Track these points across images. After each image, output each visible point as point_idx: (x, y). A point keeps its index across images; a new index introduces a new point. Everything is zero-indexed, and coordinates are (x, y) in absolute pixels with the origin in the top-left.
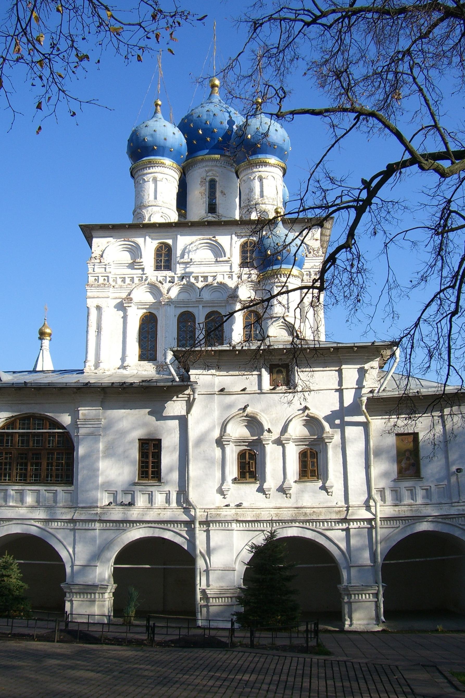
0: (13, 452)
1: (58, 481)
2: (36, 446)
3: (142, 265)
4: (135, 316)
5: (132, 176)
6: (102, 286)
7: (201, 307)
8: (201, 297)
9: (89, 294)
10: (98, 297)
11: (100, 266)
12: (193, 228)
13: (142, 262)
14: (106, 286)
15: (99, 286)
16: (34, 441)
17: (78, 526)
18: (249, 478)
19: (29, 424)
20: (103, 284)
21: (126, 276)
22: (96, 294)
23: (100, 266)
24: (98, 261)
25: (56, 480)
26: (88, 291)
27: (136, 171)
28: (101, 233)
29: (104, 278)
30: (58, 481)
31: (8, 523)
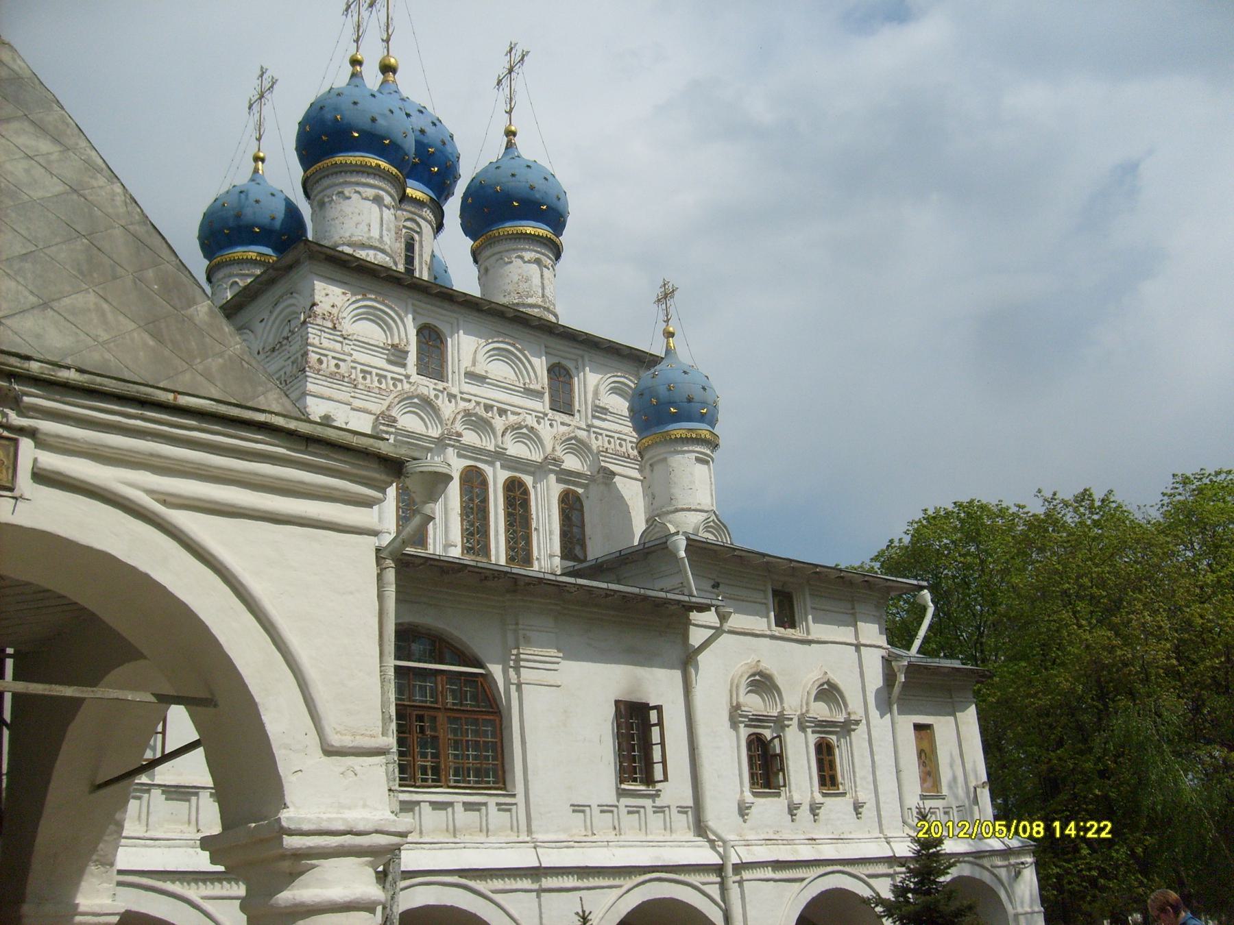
1: (488, 782)
7: (498, 464)
9: (310, 387)
10: (329, 399)
17: (549, 882)
21: (374, 371)
22: (327, 392)
24: (330, 325)
30: (488, 782)
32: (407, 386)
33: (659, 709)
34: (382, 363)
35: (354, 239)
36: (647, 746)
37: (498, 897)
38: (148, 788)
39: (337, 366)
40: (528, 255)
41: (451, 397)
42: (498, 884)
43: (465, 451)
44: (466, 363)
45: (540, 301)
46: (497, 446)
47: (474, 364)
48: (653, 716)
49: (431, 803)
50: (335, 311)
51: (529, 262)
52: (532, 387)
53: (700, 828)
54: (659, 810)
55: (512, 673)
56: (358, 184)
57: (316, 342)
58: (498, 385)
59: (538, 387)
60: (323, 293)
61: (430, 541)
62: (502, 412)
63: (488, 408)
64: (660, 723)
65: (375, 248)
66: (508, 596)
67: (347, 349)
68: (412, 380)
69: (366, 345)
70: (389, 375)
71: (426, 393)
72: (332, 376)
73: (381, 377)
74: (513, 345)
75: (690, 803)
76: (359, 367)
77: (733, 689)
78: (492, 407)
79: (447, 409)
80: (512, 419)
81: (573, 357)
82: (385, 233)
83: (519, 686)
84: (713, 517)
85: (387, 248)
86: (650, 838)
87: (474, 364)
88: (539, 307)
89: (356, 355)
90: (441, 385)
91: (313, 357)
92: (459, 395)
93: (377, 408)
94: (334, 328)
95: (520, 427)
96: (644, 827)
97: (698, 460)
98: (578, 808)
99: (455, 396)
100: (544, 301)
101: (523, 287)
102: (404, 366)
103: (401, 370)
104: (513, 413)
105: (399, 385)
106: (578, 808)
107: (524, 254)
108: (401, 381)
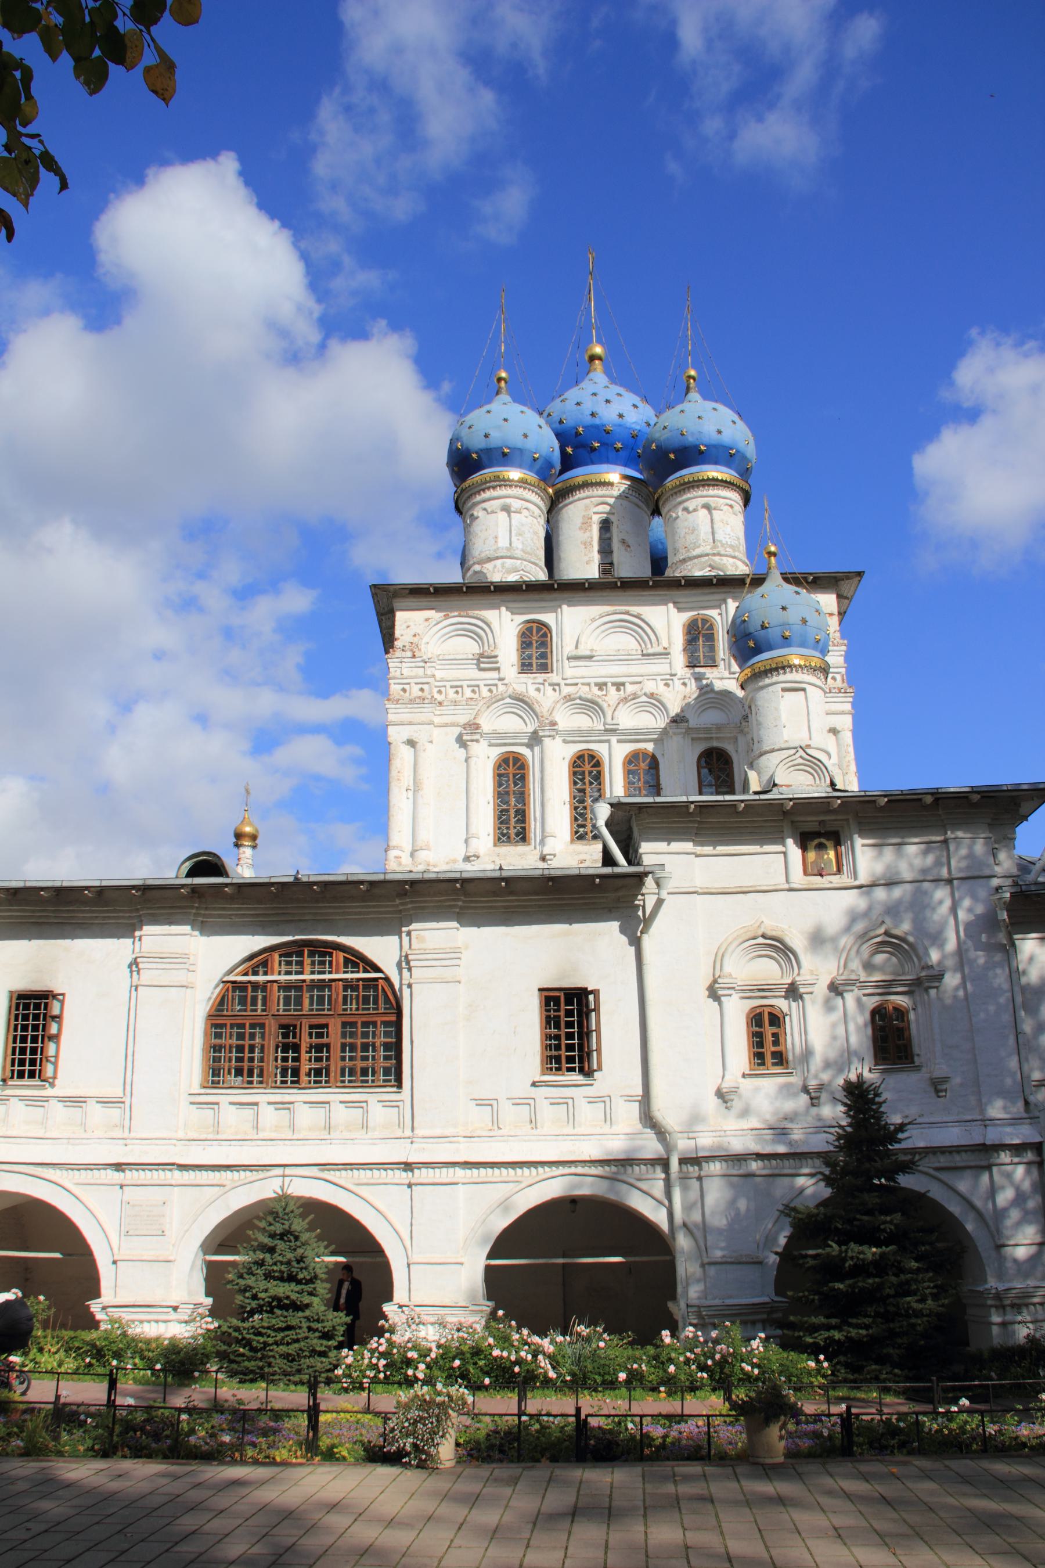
0: (267, 1022)
2: (317, 1010)
3: (497, 662)
4: (485, 758)
5: (459, 510)
6: (418, 701)
8: (614, 722)
9: (391, 717)
10: (410, 724)
11: (413, 665)
12: (591, 594)
13: (496, 657)
14: (426, 701)
15: (411, 701)
16: (311, 997)
18: (774, 1064)
19: (301, 963)
20: (419, 697)
21: (465, 684)
22: (406, 717)
23: (413, 665)
24: (409, 654)
25: (362, 1081)
26: (390, 711)
27: (467, 495)
28: (412, 601)
29: (420, 686)
31: (261, 1175)
32: (501, 688)
33: (596, 993)
34: (474, 673)
35: (483, 555)
36: (585, 1034)
37: (363, 1191)
38: (46, 1099)
39: (422, 690)
40: (691, 505)
41: (555, 686)
42: (364, 1175)
43: (570, 737)
44: (569, 649)
45: (707, 549)
46: (605, 724)
47: (577, 647)
48: (591, 997)
49: (305, 1103)
50: (415, 640)
51: (695, 510)
52: (650, 651)
53: (648, 1119)
54: (592, 1100)
55: (405, 972)
56: (484, 501)
57: (398, 674)
58: (608, 660)
59: (660, 650)
60: (404, 626)
61: (532, 835)
62: (619, 686)
63: (601, 686)
64: (597, 1009)
65: (497, 558)
66: (398, 901)
67: (429, 672)
68: (505, 682)
69: (454, 661)
70: (481, 683)
71: (520, 689)
72: (411, 701)
73: (475, 688)
74: (627, 613)
75: (639, 1091)
76: (448, 684)
77: (719, 960)
78: (605, 684)
79: (546, 699)
80: (630, 689)
81: (718, 603)
82: (514, 539)
83: (410, 986)
84: (801, 753)
85: (518, 553)
86: (575, 1132)
87: (577, 647)
88: (707, 555)
89: (439, 674)
90: (540, 677)
91: (395, 688)
92: (562, 682)
93: (463, 719)
94: (414, 656)
95: (635, 696)
96: (572, 1118)
97: (784, 690)
98: (480, 1102)
99: (558, 685)
100: (714, 547)
101: (691, 538)
102: (498, 669)
103: (494, 675)
104: (631, 683)
105: (494, 688)
106: (480, 1102)
107: (686, 504)
108: (496, 685)
